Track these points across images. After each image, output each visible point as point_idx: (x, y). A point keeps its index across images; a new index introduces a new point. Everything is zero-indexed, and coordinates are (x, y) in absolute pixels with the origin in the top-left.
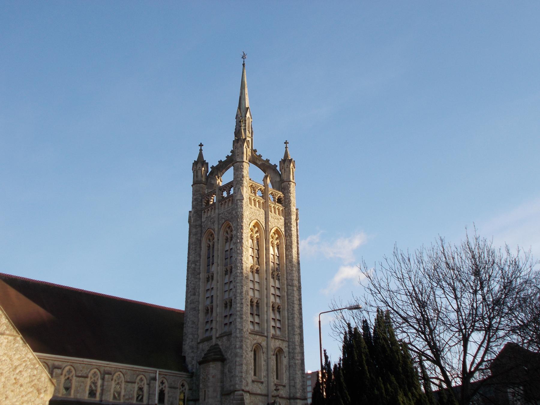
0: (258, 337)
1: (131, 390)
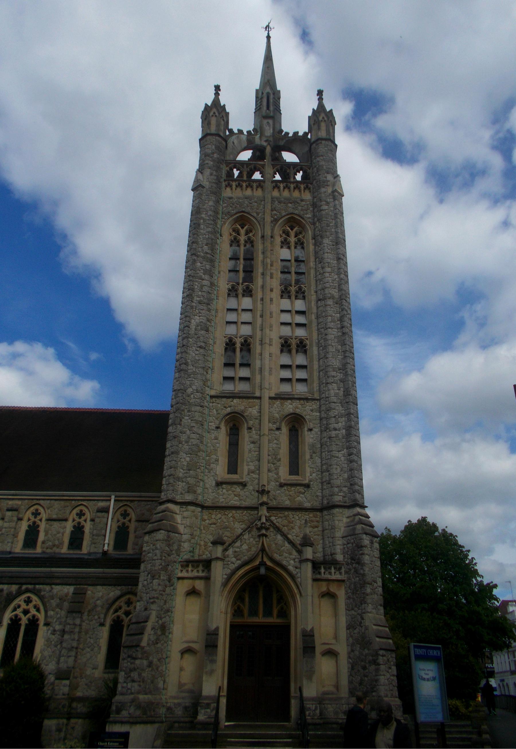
0: (235, 401)
1: (58, 533)
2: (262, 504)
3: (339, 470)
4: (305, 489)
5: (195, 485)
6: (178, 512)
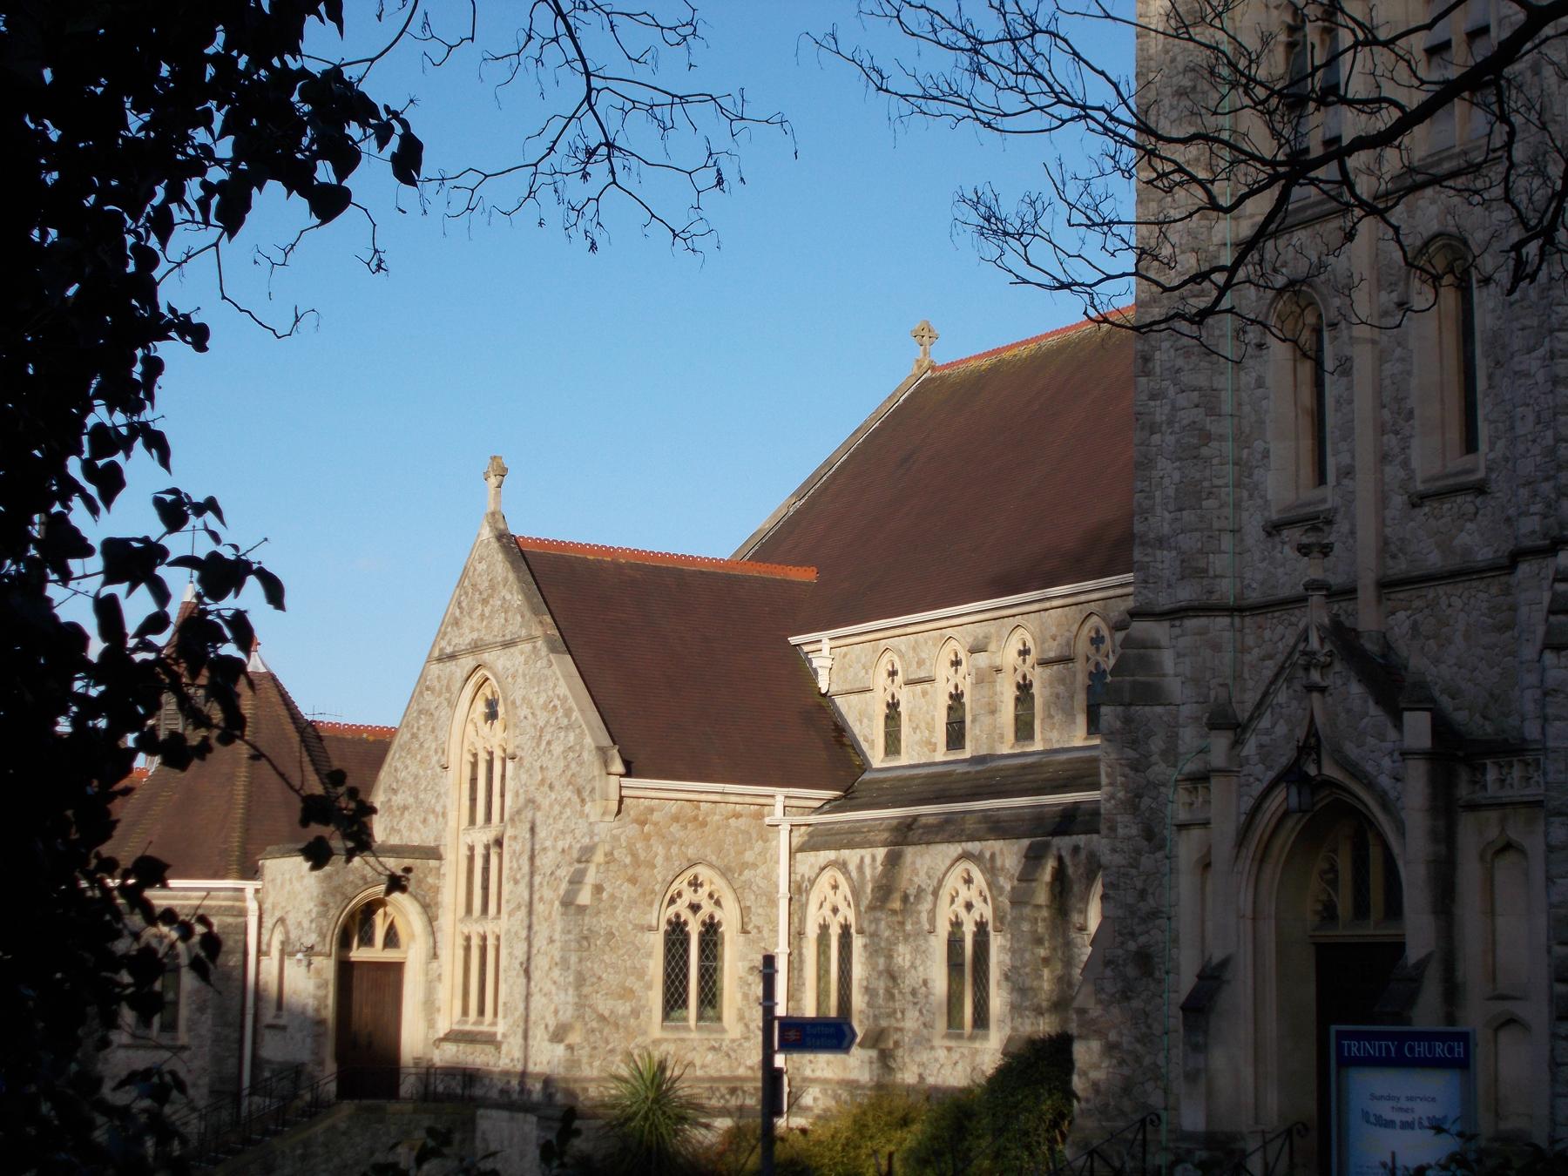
2: (1313, 586)
3: (1531, 418)
4: (1478, 501)
5: (1200, 551)
6: (1164, 641)
